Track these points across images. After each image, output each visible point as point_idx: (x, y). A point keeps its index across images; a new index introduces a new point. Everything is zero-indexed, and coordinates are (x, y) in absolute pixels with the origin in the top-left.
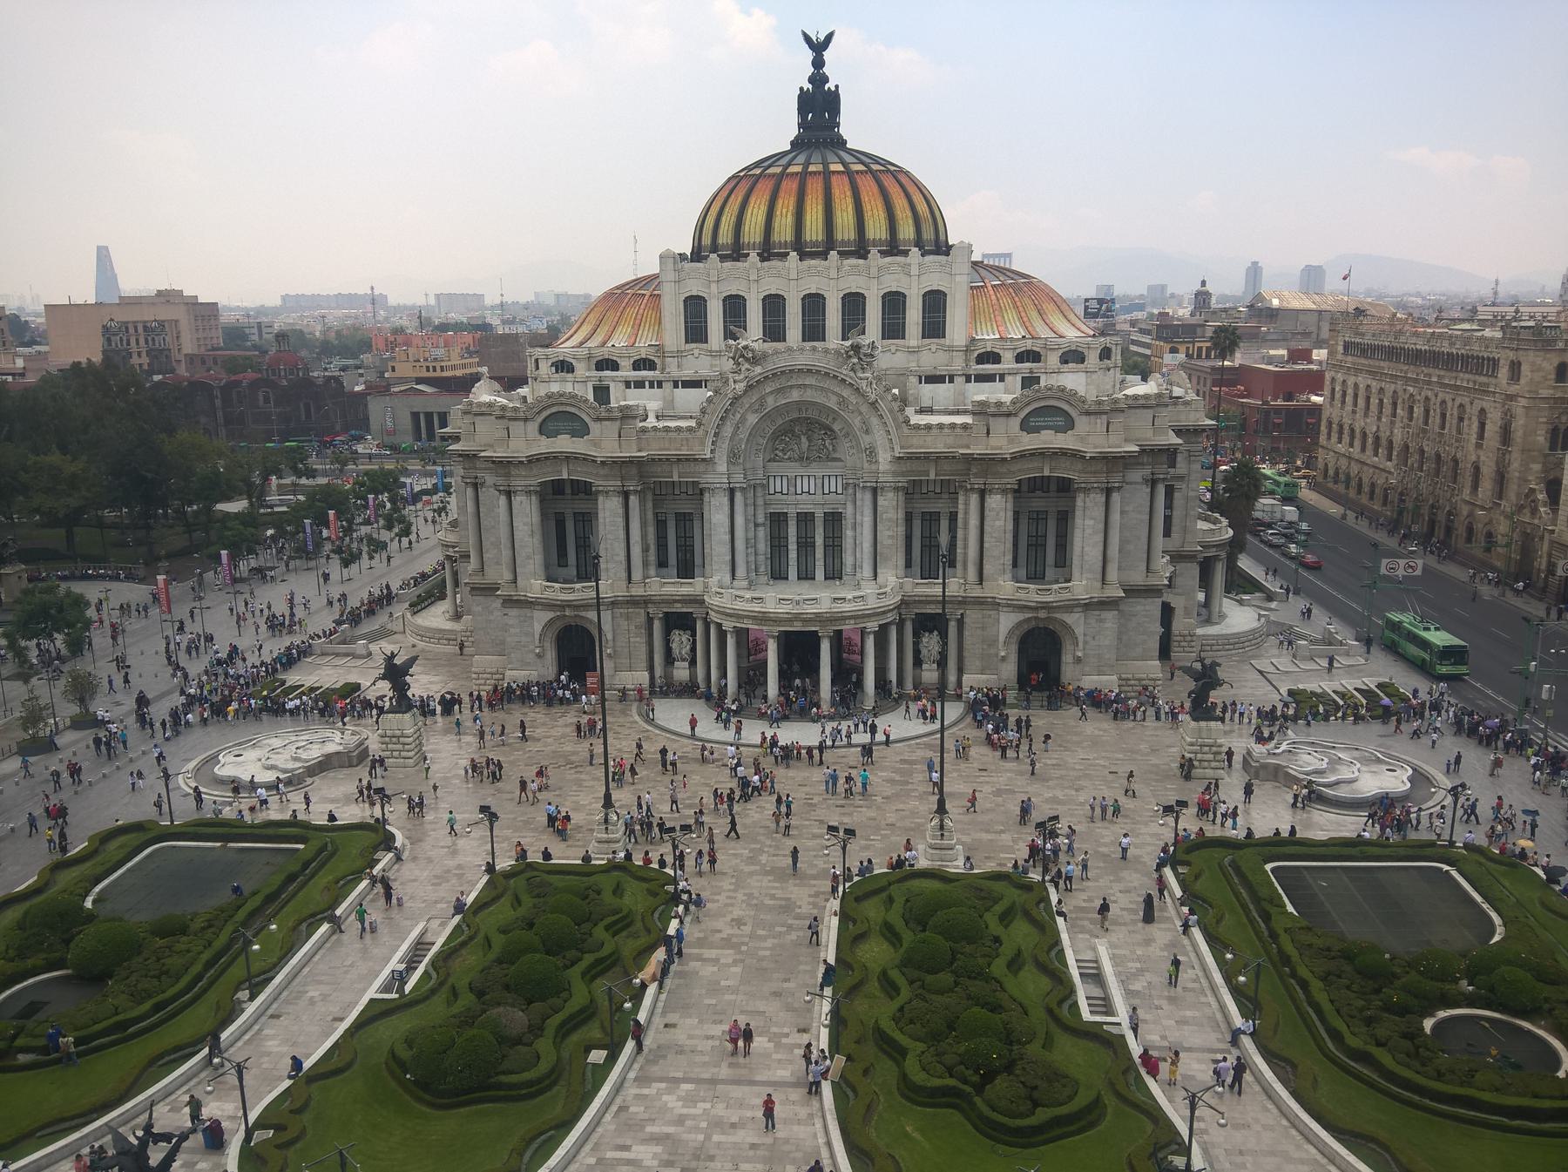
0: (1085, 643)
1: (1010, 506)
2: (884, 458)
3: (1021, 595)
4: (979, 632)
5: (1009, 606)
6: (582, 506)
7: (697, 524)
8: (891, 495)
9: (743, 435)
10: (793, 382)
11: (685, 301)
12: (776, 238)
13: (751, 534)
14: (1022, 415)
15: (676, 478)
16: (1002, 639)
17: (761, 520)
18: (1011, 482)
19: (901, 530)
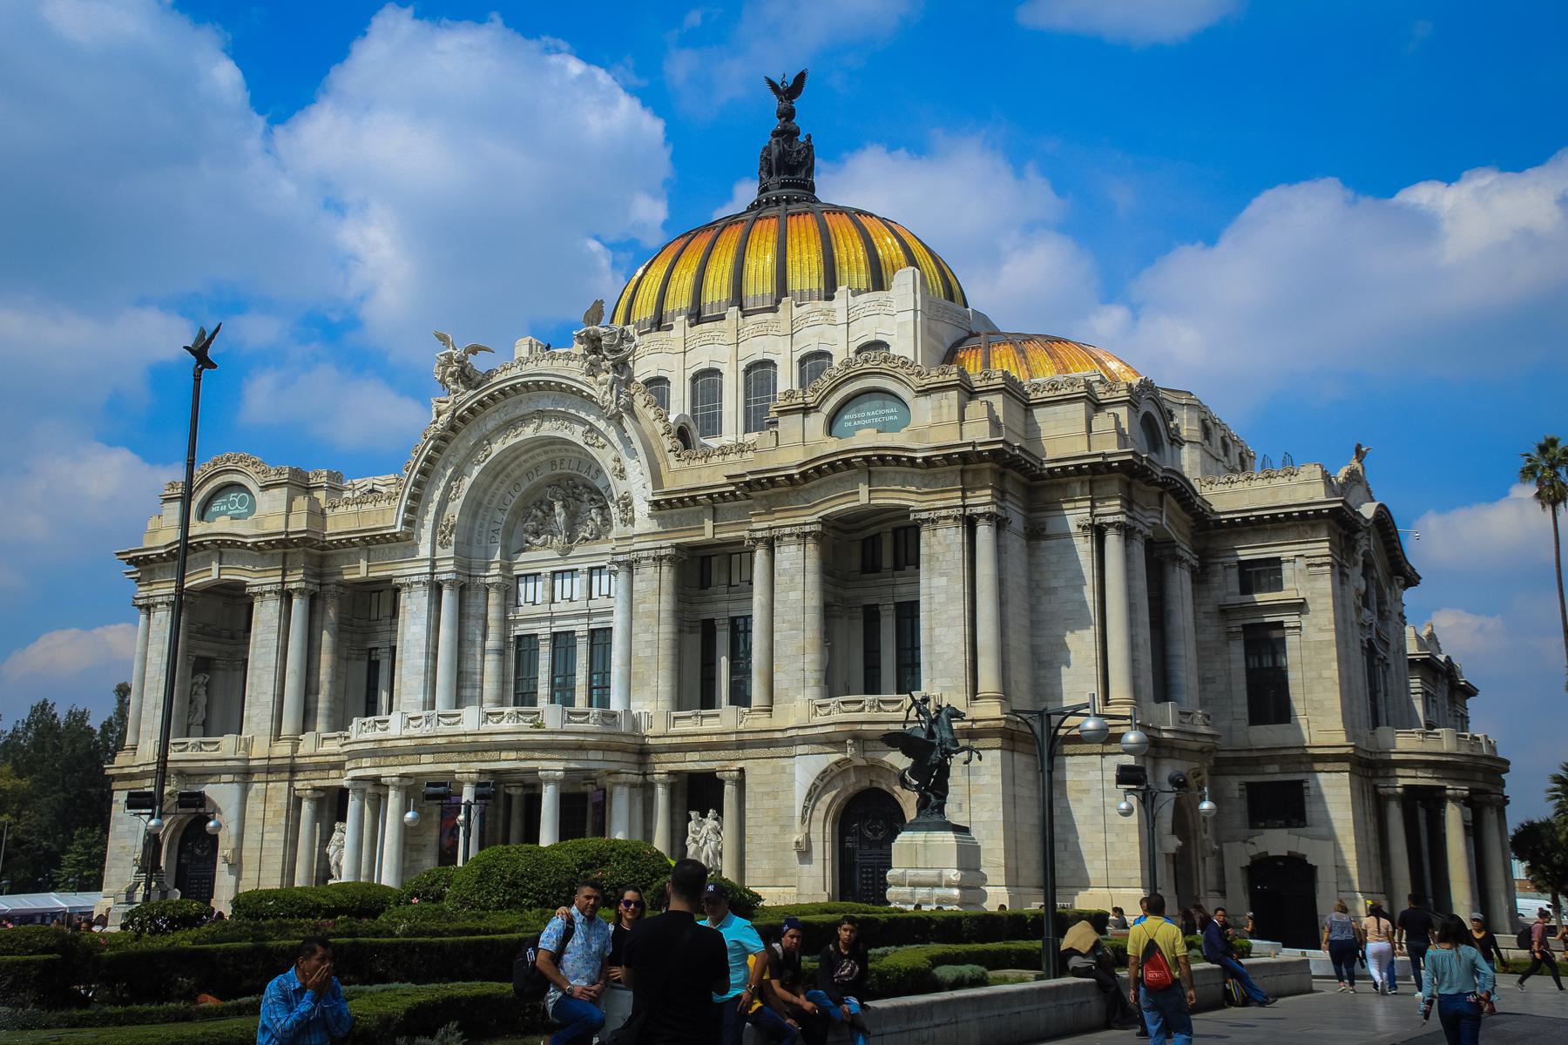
2: (642, 509)
4: (768, 803)
5: (806, 741)
9: (459, 502)
12: (668, 307)
14: (828, 407)
17: (492, 643)
18: (810, 517)
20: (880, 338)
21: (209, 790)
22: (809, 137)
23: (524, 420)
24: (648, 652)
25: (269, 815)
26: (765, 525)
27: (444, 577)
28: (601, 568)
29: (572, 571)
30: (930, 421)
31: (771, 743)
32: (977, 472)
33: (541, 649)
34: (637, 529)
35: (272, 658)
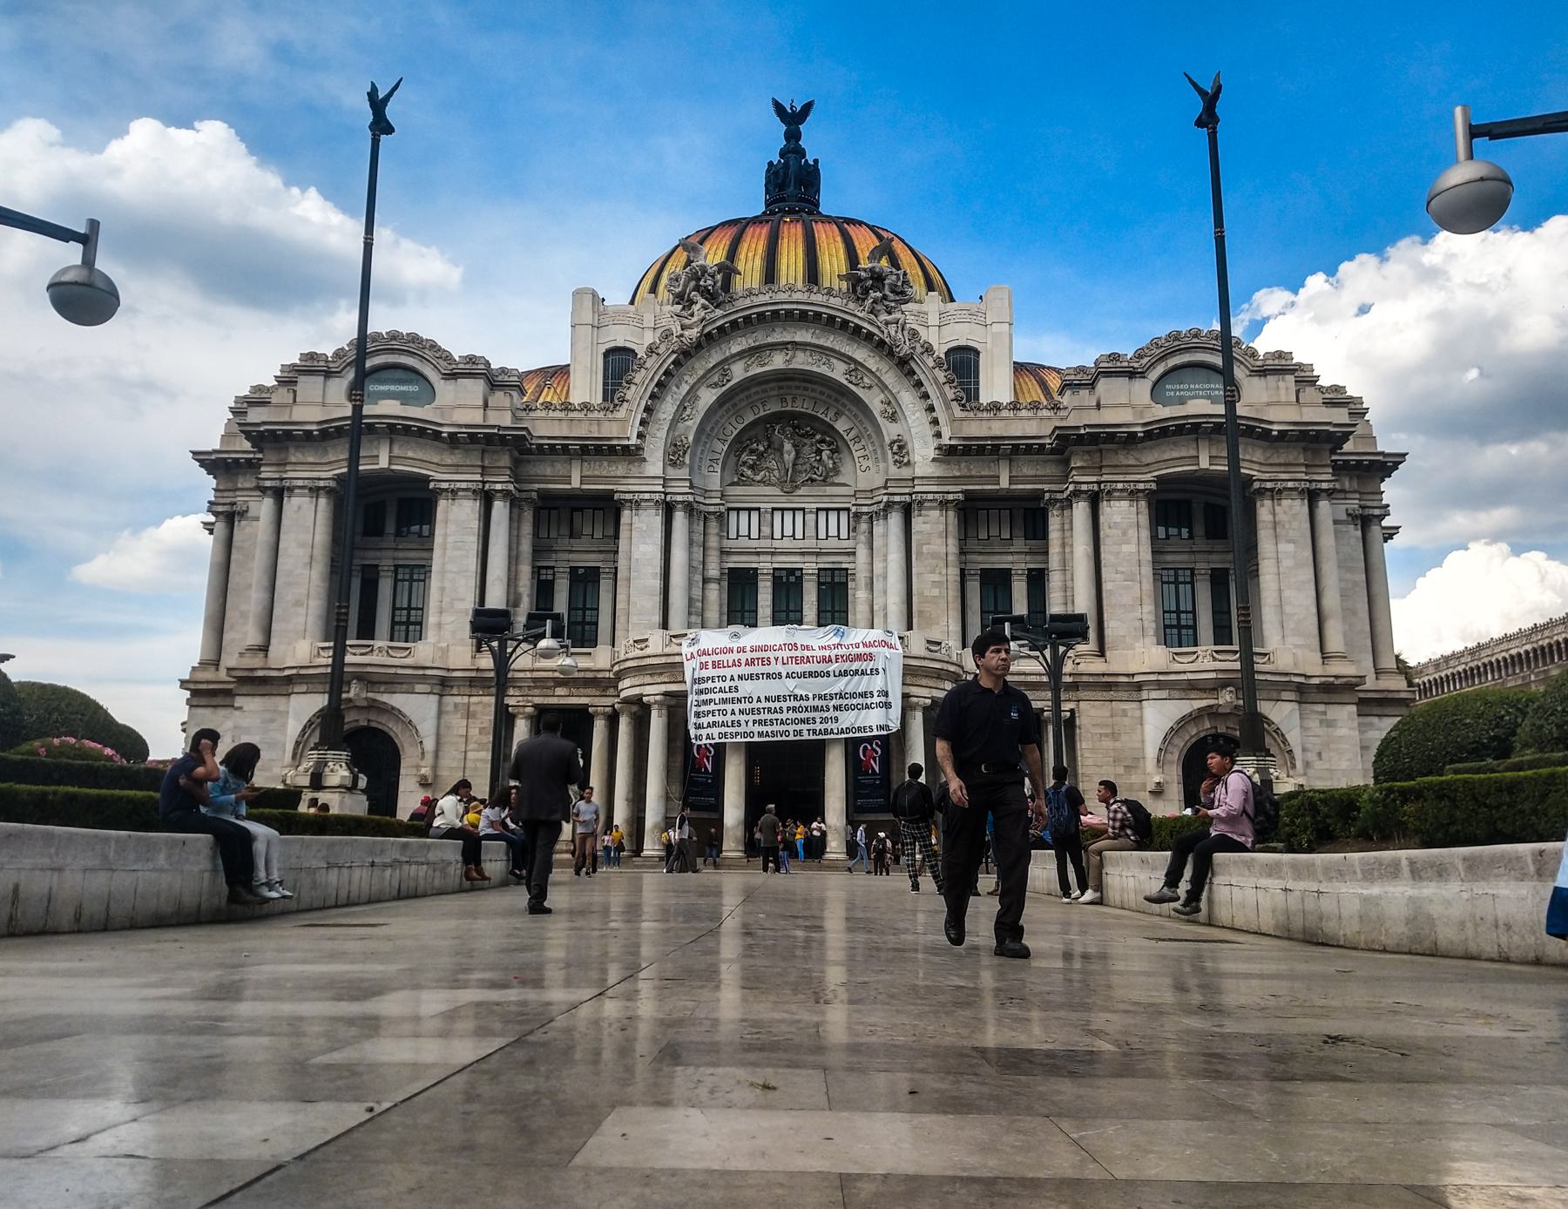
0: (1307, 764)
1: (1144, 519)
2: (923, 454)
3: (1183, 664)
4: (1107, 743)
5: (1160, 685)
6: (412, 557)
7: (605, 585)
8: (935, 514)
9: (693, 424)
10: (778, 336)
11: (607, 353)
13: (697, 592)
15: (576, 483)
16: (1151, 752)
17: (713, 572)
18: (1146, 479)
19: (954, 572)
20: (971, 344)
21: (396, 700)
22: (816, 161)
23: (773, 347)
24: (936, 592)
25: (474, 732)
26: (1094, 479)
27: (680, 498)
28: (827, 510)
29: (794, 510)
30: (1265, 399)
31: (1109, 686)
32: (1316, 452)
33: (760, 584)
34: (919, 472)
35: (472, 563)
